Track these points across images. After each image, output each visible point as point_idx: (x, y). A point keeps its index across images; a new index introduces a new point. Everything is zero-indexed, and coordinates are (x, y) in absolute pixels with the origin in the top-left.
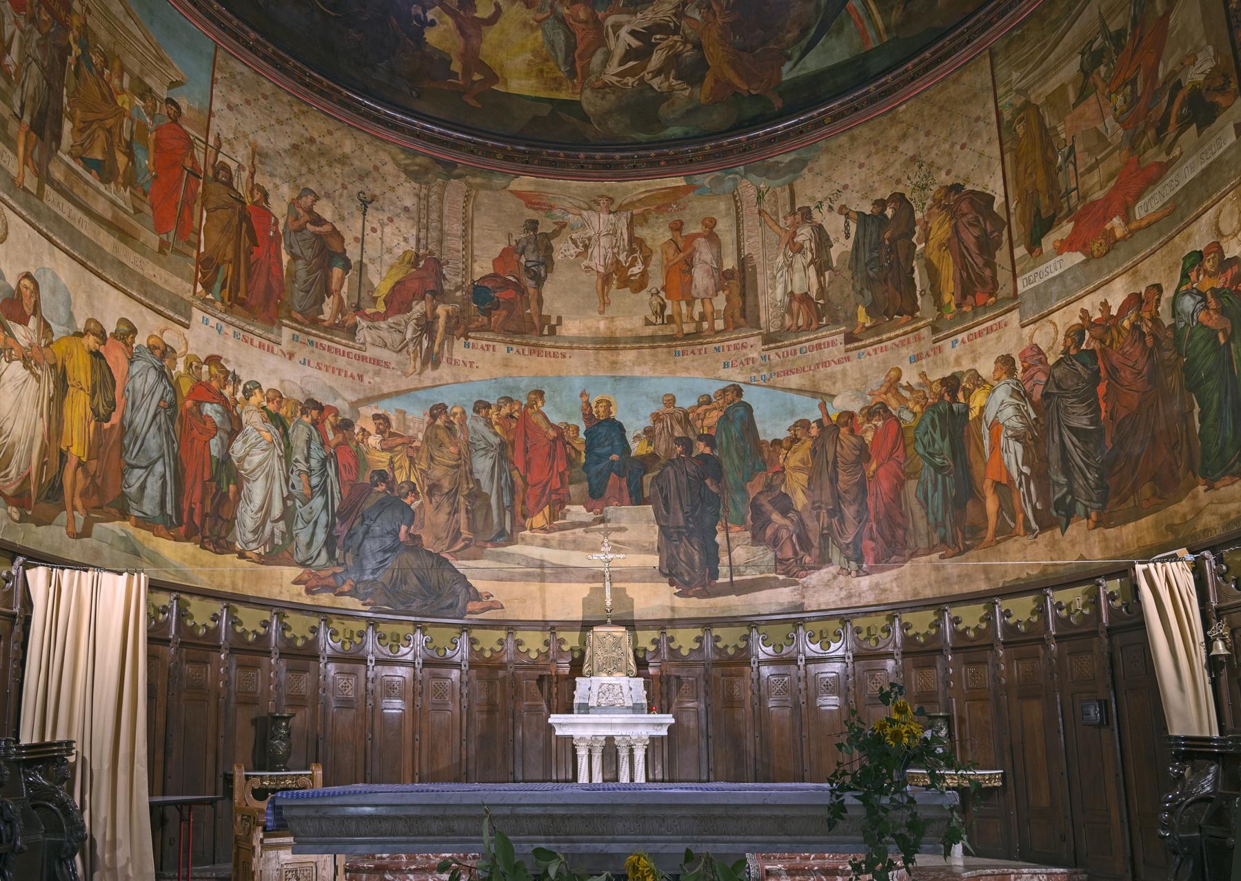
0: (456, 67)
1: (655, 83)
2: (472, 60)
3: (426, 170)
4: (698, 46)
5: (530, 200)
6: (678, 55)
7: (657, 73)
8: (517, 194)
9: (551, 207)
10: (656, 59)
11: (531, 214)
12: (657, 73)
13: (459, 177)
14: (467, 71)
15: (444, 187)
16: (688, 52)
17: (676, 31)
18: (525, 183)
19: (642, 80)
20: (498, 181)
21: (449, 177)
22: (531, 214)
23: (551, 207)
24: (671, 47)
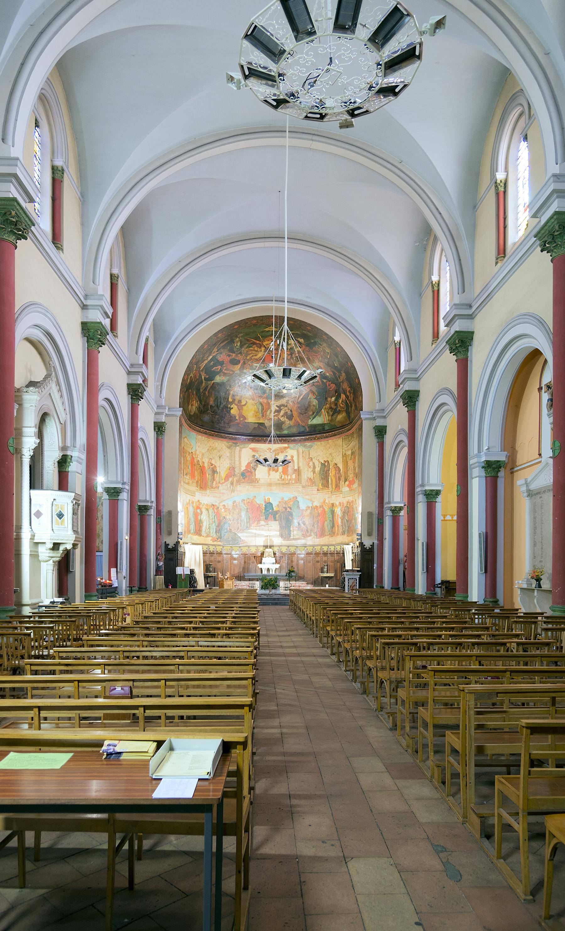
0: (237, 418)
1: (282, 419)
2: (241, 416)
3: (231, 446)
4: (291, 411)
5: (253, 450)
6: (287, 412)
7: (282, 416)
8: (251, 448)
9: (258, 451)
10: (282, 413)
11: (254, 454)
12: (282, 416)
13: (238, 446)
14: (239, 418)
15: (235, 449)
16: (289, 412)
17: (286, 406)
18: (253, 445)
19: (279, 418)
20: (246, 445)
21: (236, 446)
22: (254, 454)
23: (258, 451)
24: (285, 410)
